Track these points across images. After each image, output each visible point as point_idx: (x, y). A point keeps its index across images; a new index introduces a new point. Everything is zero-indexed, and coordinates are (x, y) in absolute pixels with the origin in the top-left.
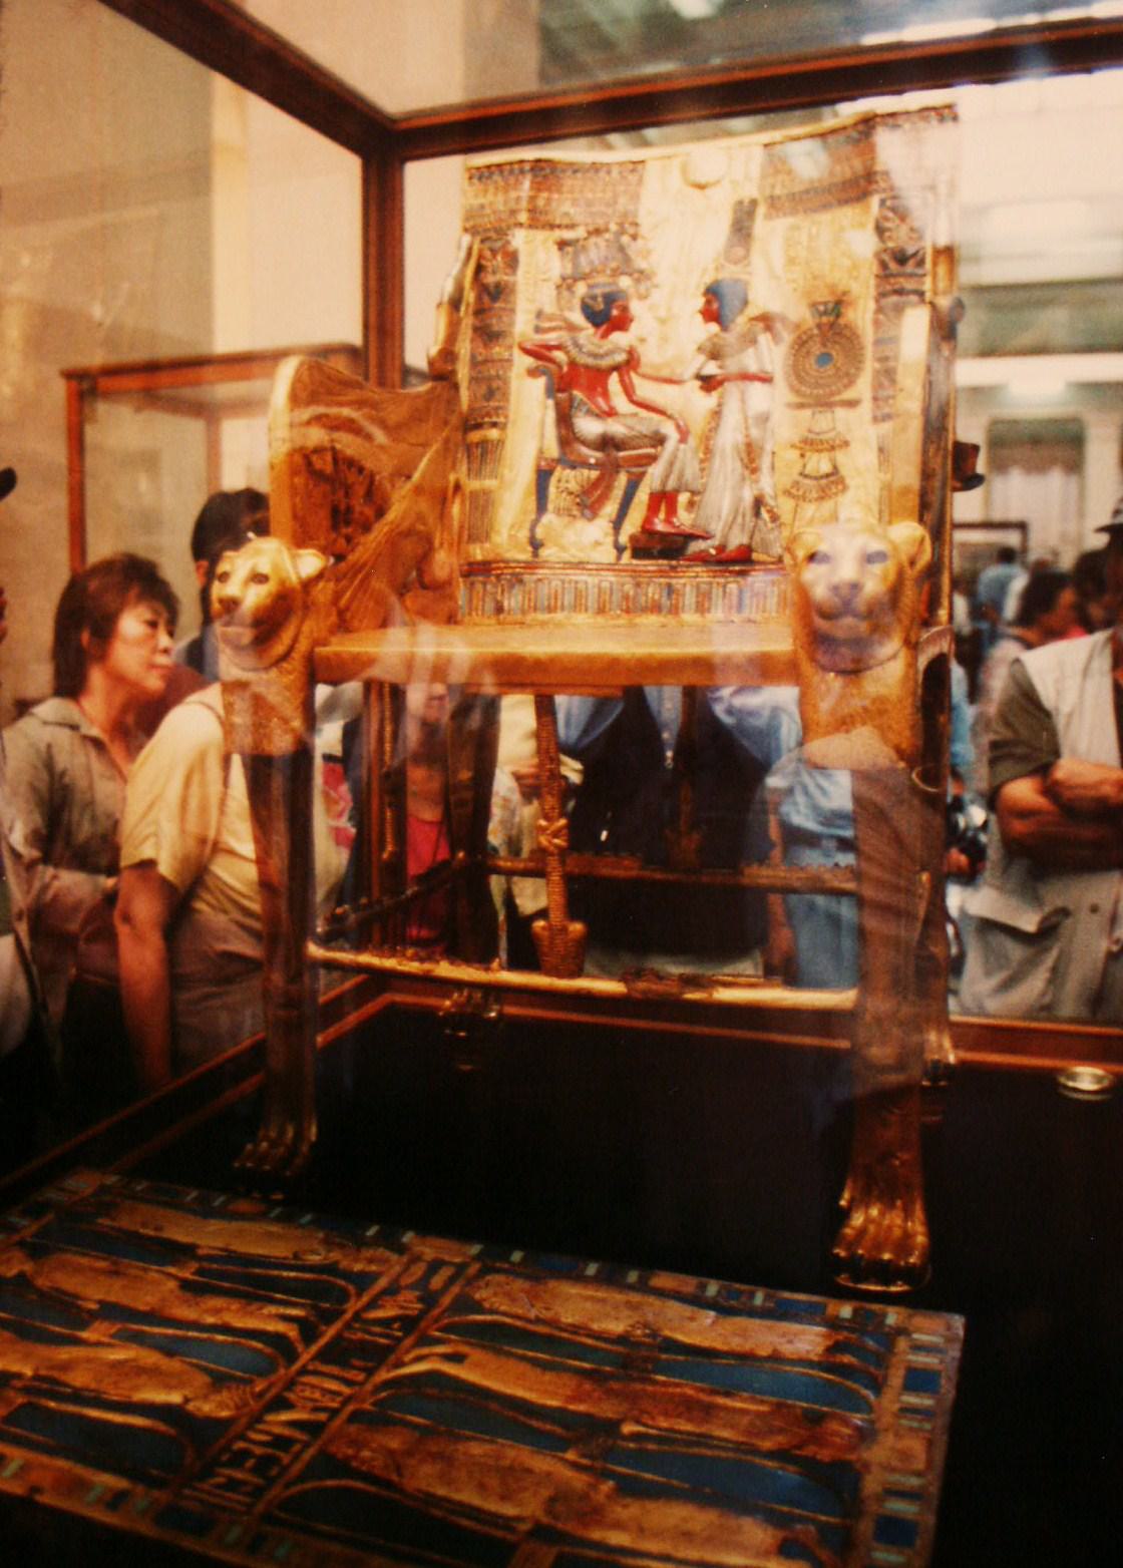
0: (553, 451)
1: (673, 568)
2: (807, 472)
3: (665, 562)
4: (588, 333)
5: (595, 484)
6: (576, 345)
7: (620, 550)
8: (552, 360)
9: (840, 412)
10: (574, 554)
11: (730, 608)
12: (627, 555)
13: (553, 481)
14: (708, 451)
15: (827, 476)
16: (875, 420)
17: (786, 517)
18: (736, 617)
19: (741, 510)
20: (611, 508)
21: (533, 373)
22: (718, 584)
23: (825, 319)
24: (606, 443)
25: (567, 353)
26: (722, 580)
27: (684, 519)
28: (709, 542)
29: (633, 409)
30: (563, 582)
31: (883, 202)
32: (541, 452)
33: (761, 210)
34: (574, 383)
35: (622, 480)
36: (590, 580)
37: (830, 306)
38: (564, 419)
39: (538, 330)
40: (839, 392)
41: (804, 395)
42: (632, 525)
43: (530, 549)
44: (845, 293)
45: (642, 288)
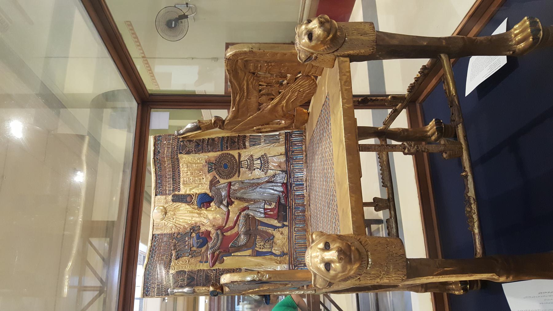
0: (249, 252)
1: (290, 207)
4: (210, 244)
5: (261, 236)
6: (212, 248)
7: (284, 226)
8: (218, 255)
10: (285, 241)
12: (285, 223)
13: (260, 250)
15: (261, 161)
18: (305, 186)
20: (270, 230)
21: (222, 262)
23: (213, 167)
24: (248, 233)
25: (216, 250)
27: (273, 205)
30: (295, 244)
31: (180, 153)
32: (250, 256)
33: (177, 193)
34: (227, 247)
35: (260, 227)
36: (294, 235)
37: (210, 166)
38: (239, 249)
39: (206, 262)
41: (236, 171)
42: (275, 222)
44: (206, 162)
45: (196, 229)
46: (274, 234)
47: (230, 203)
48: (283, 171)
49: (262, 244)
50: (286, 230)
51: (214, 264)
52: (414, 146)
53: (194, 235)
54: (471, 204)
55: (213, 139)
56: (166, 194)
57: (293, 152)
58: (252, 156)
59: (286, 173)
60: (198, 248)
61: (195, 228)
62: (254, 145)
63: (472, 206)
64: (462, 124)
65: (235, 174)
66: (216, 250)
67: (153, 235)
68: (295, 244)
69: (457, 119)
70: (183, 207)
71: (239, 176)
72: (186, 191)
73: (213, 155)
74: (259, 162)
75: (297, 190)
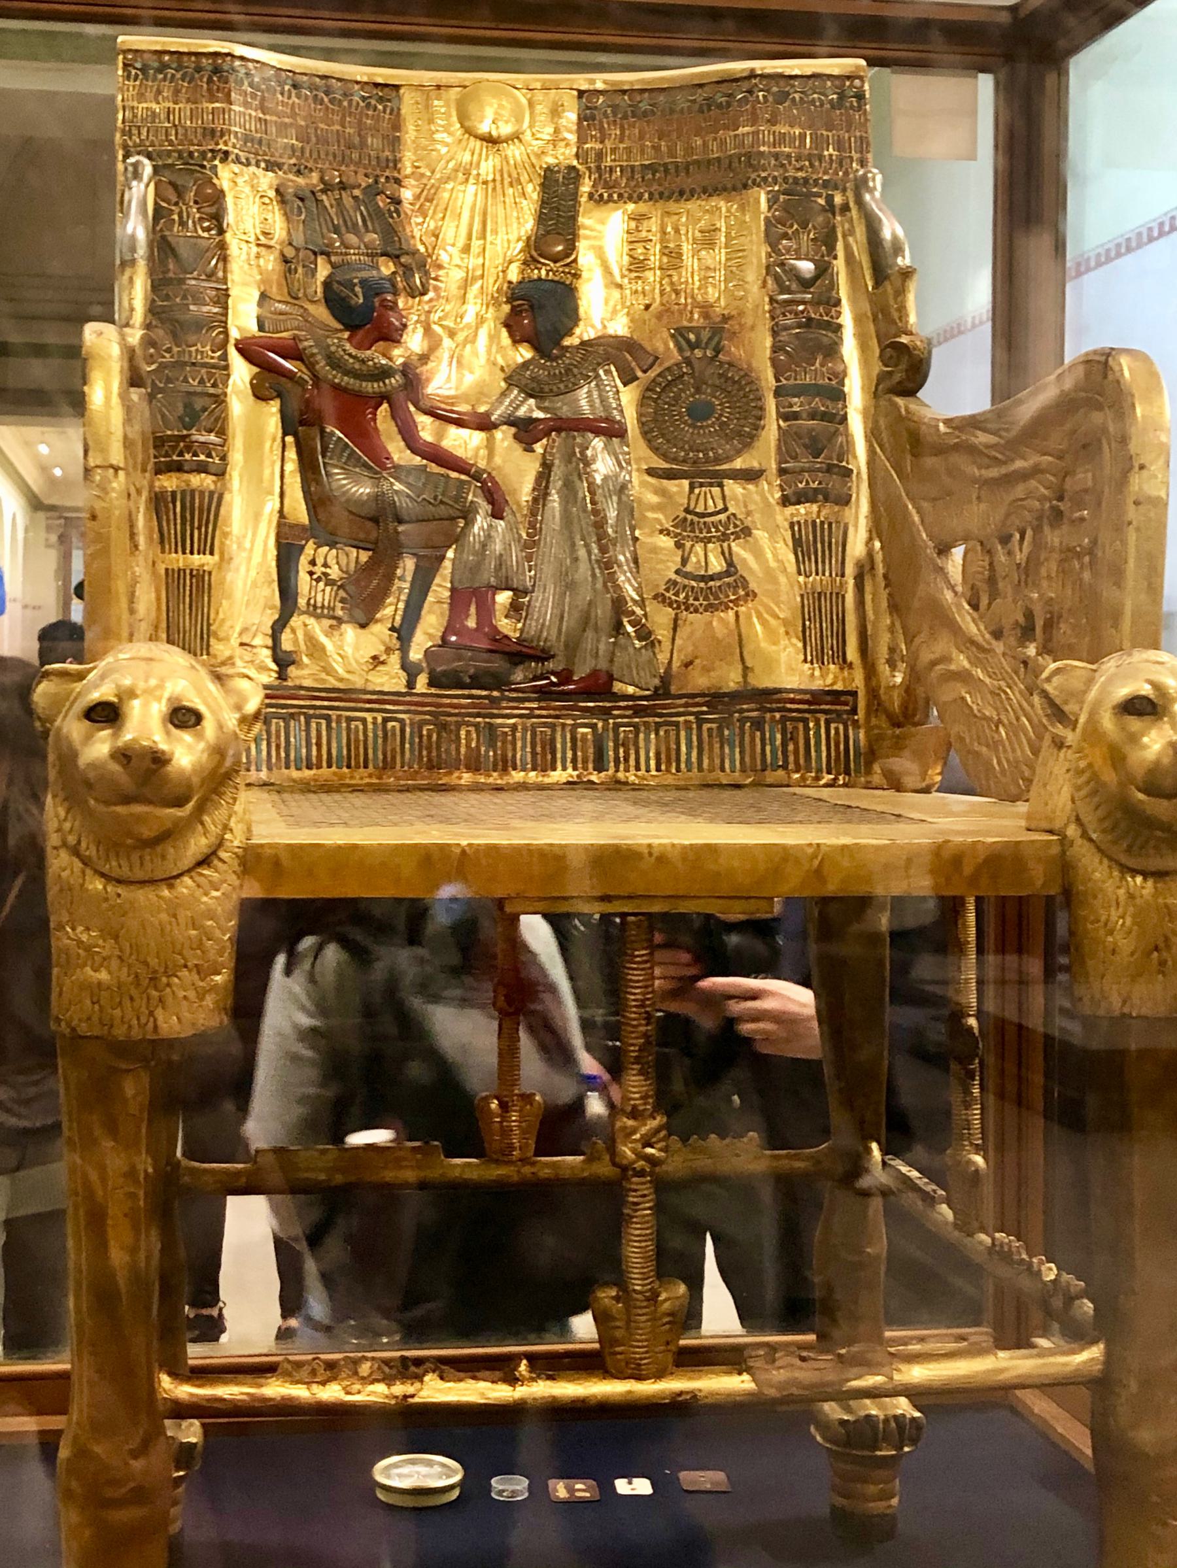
2: (688, 568)
3: (484, 693)
9: (733, 487)
11: (585, 761)
13: (303, 561)
14: (534, 527)
16: (785, 501)
17: (662, 633)
19: (593, 621)
20: (392, 609)
22: (564, 725)
23: (698, 353)
25: (311, 367)
26: (570, 722)
28: (550, 665)
29: (417, 460)
30: (328, 718)
33: (586, 187)
36: (369, 717)
37: (705, 335)
40: (729, 459)
41: (674, 460)
43: (274, 667)
44: (726, 319)
46: (376, 628)
47: (526, 432)
48: (666, 680)
49: (334, 573)
50: (391, 679)
51: (246, 350)
52: (649, 1159)
53: (387, 268)
54: (388, 1380)
55: (832, 351)
56: (581, 140)
57: (758, 724)
58: (747, 532)
59: (656, 695)
60: (327, 284)
61: (416, 270)
62: (797, 543)
63: (381, 1388)
64: (750, 1394)
65: (665, 457)
66: (311, 367)
67: (397, 87)
68: (328, 718)
69: (779, 1375)
70: (518, 221)
71: (651, 472)
72: (586, 228)
73: (758, 350)
74: (717, 565)
75: (574, 740)
